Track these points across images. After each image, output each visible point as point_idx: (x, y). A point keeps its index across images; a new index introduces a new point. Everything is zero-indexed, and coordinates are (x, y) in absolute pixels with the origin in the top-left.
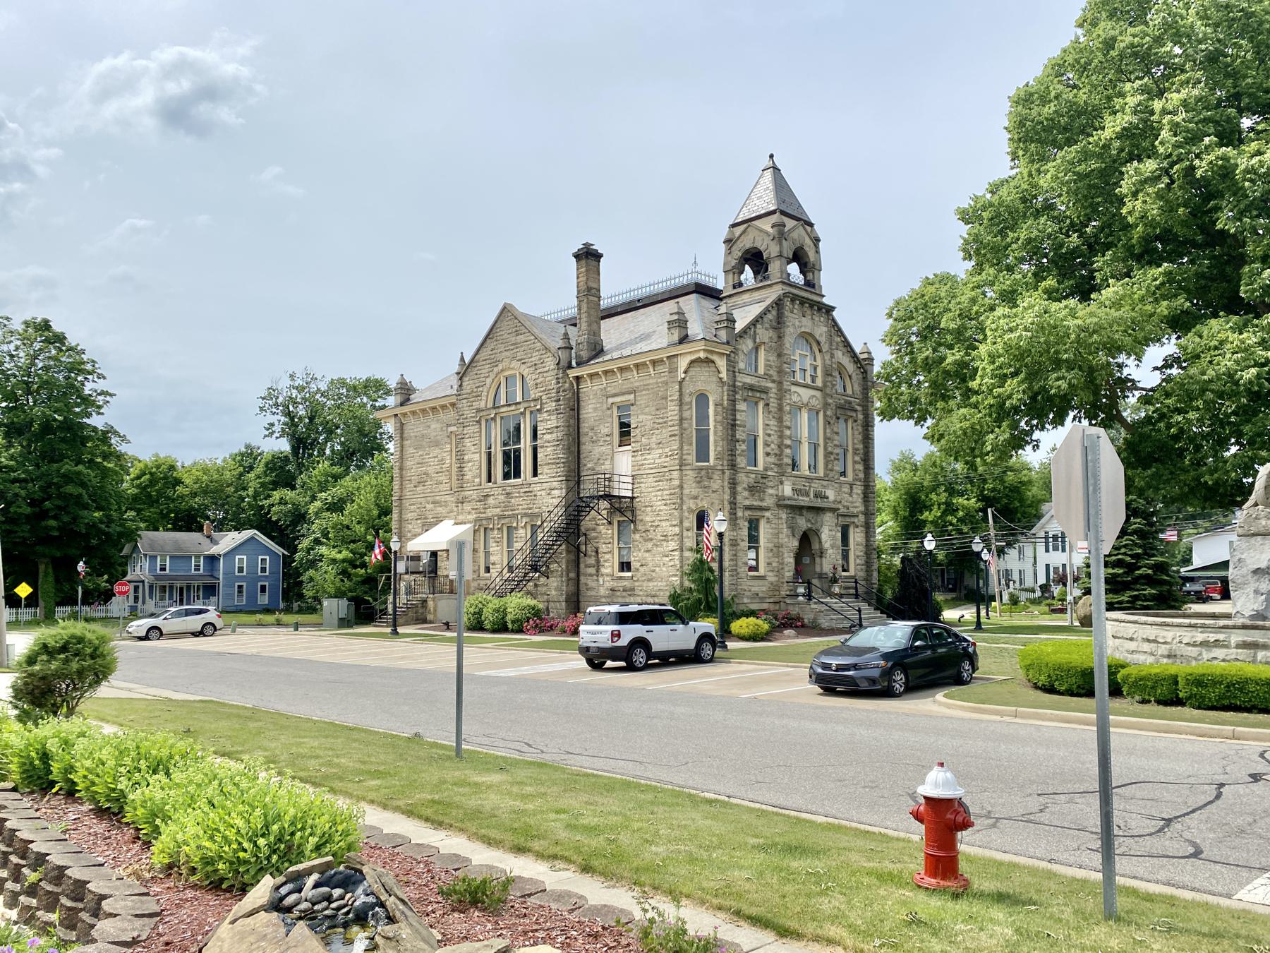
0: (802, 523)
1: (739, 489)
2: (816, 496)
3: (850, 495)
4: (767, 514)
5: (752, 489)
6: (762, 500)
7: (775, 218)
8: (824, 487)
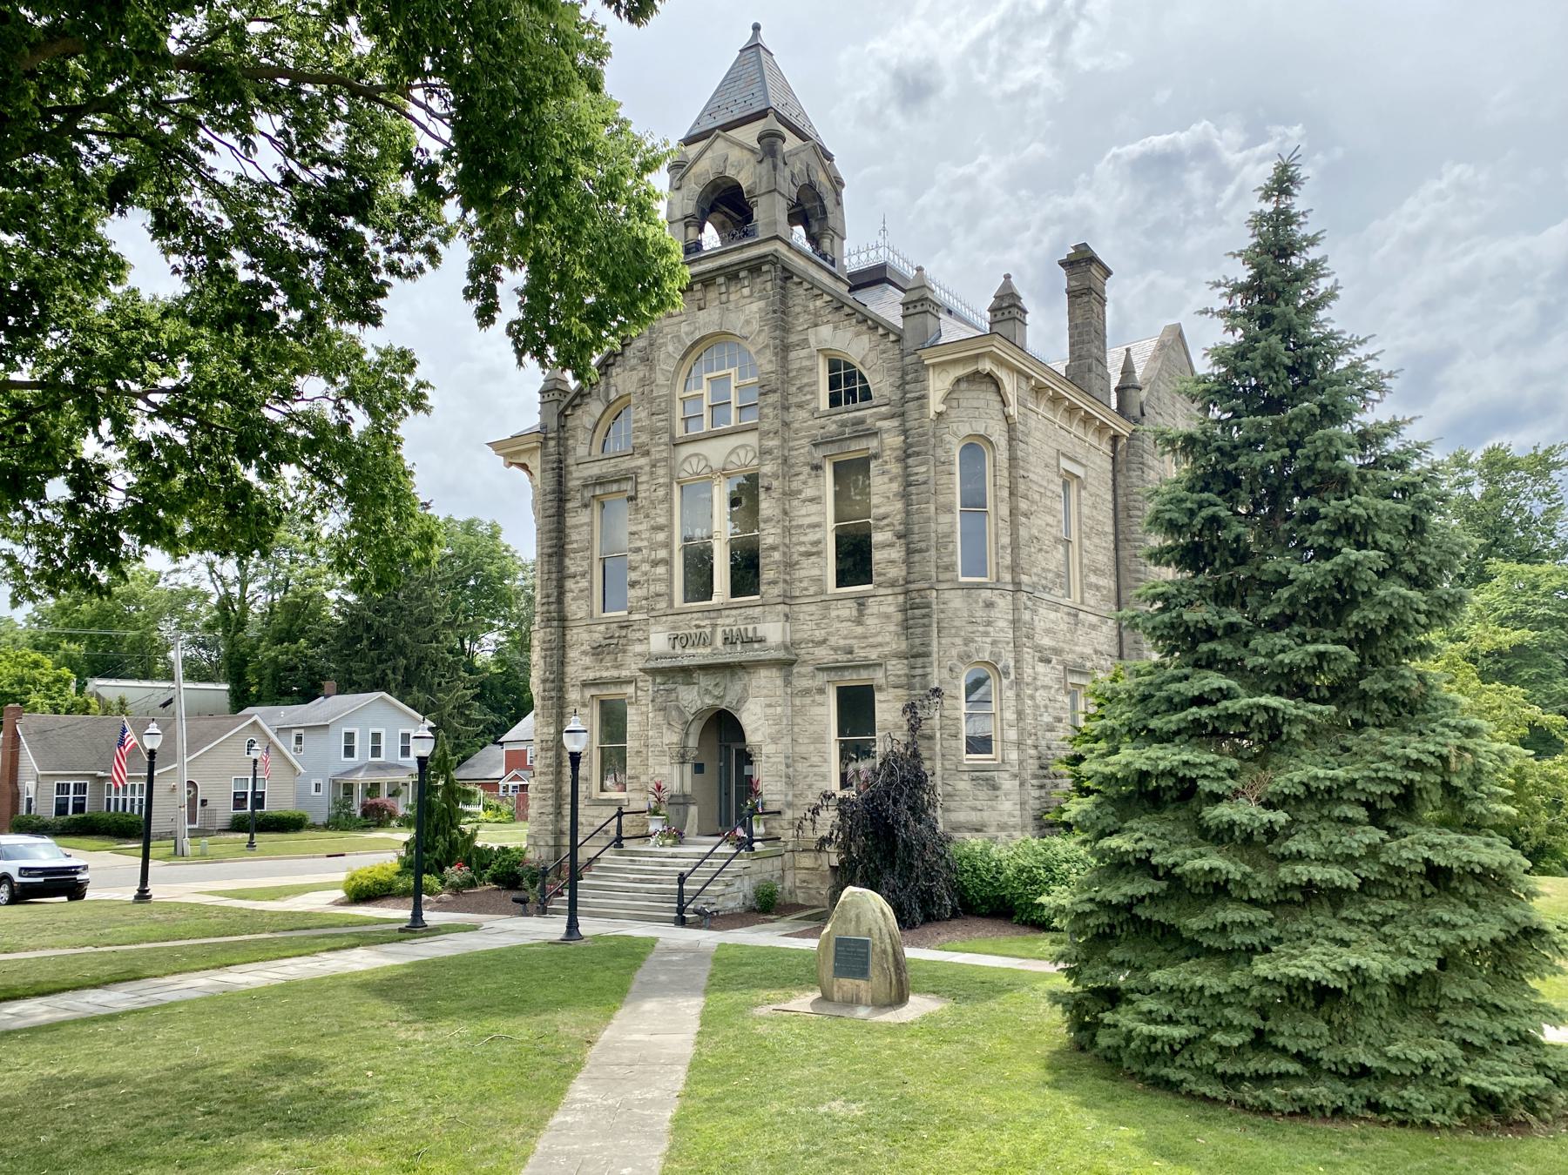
0: (693, 698)
1: (572, 654)
2: (727, 640)
3: (859, 621)
4: (630, 690)
5: (598, 651)
6: (617, 667)
7: (758, 127)
8: (754, 619)
